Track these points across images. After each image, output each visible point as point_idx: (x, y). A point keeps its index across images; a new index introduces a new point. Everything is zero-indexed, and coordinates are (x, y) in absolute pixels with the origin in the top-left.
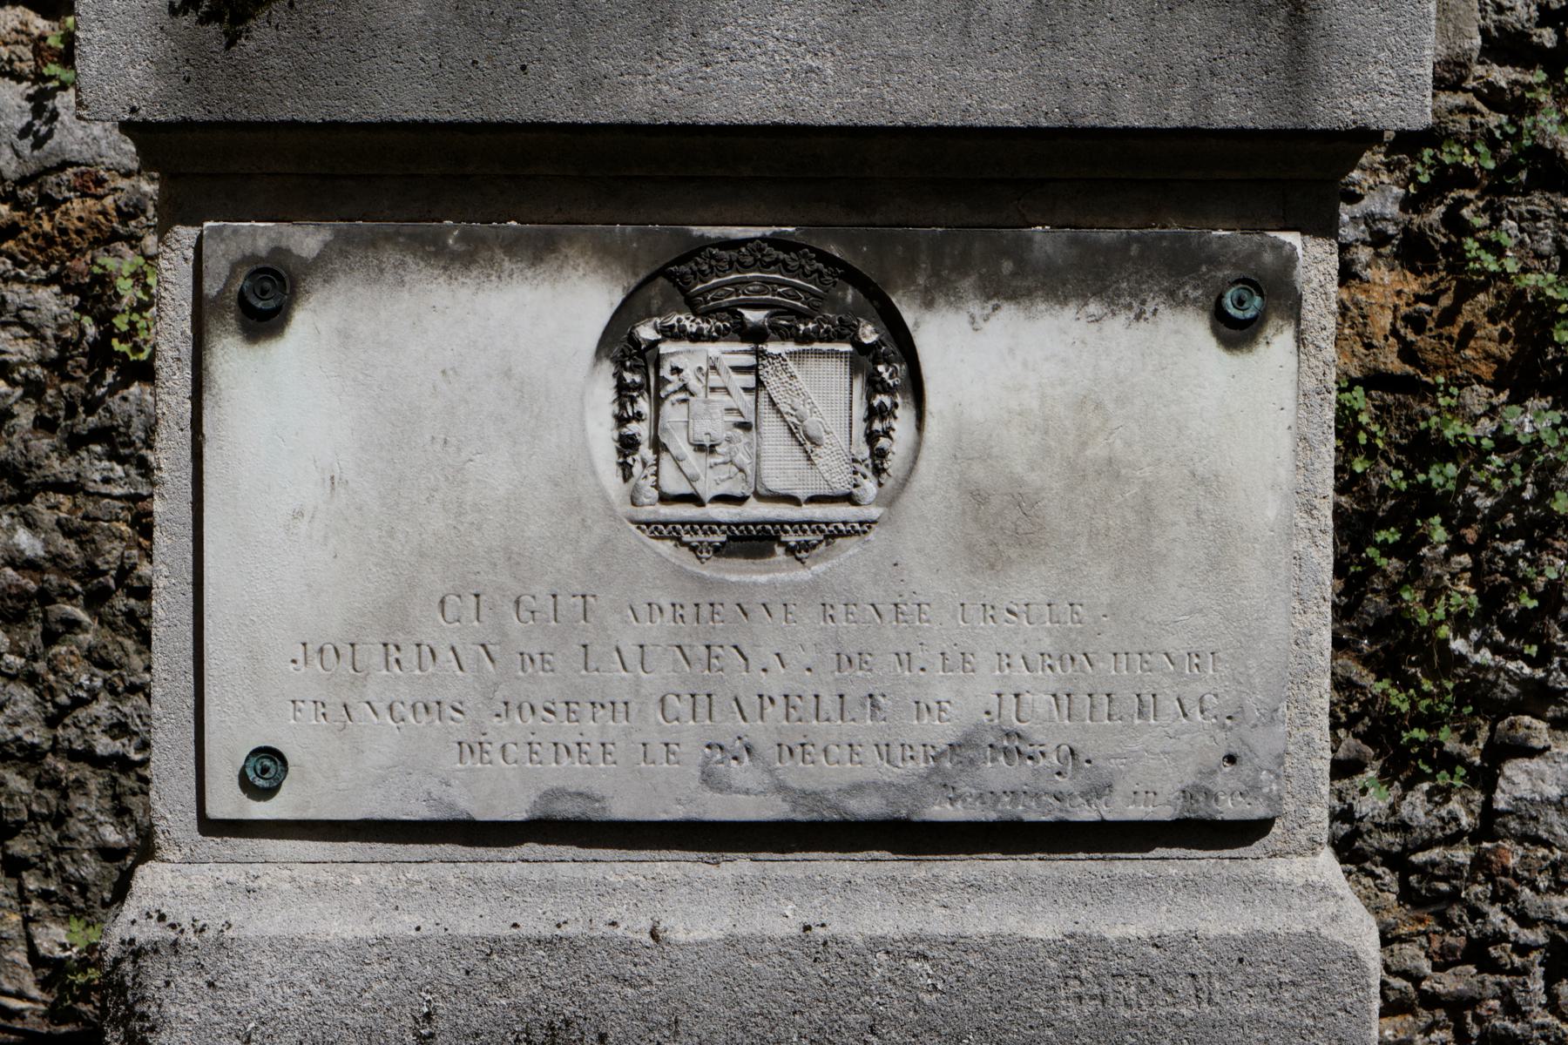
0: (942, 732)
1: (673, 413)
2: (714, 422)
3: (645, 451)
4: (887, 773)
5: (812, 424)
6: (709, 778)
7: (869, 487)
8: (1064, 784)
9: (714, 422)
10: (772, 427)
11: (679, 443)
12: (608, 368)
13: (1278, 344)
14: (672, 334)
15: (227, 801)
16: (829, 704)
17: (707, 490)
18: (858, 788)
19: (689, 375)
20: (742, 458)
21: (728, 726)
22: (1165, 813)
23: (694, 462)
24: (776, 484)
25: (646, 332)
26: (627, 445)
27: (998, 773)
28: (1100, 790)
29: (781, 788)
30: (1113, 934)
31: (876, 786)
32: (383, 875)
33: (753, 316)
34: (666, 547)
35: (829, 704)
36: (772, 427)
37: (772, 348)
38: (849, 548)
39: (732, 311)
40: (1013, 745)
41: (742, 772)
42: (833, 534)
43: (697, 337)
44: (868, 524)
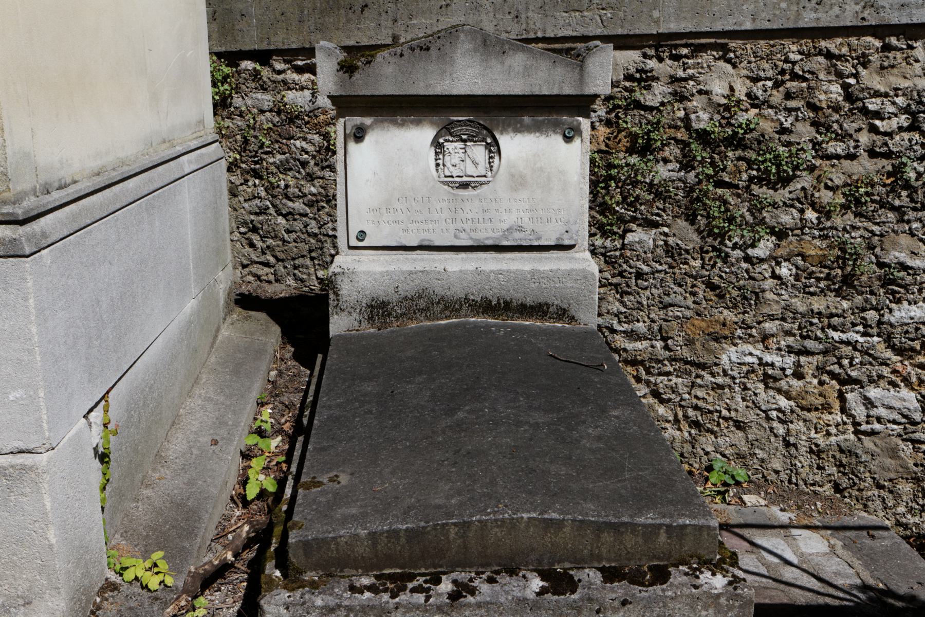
0: (505, 226)
1: (447, 158)
2: (456, 160)
3: (441, 166)
4: (493, 235)
5: (477, 160)
6: (456, 236)
7: (489, 174)
8: (531, 237)
9: (456, 160)
10: (468, 161)
11: (448, 164)
12: (433, 148)
13: (577, 142)
14: (447, 141)
15: (354, 242)
16: (481, 220)
17: (455, 175)
18: (487, 238)
19: (450, 150)
20: (462, 168)
21: (460, 225)
22: (553, 243)
23: (452, 168)
24: (469, 173)
25: (441, 141)
26: (438, 165)
27: (517, 235)
28: (539, 238)
29: (471, 238)
30: (542, 269)
31: (491, 238)
32: (387, 258)
33: (464, 137)
34: (446, 187)
35: (481, 220)
36: (468, 161)
37: (468, 144)
38: (485, 187)
39: (459, 136)
40: (520, 229)
41: (463, 235)
42: (482, 184)
43: (452, 141)
44: (489, 182)
